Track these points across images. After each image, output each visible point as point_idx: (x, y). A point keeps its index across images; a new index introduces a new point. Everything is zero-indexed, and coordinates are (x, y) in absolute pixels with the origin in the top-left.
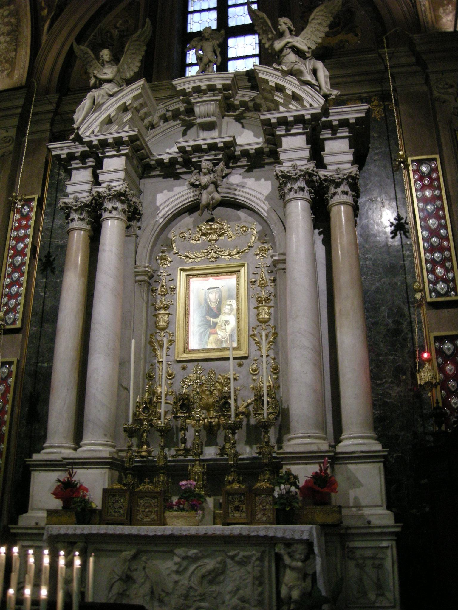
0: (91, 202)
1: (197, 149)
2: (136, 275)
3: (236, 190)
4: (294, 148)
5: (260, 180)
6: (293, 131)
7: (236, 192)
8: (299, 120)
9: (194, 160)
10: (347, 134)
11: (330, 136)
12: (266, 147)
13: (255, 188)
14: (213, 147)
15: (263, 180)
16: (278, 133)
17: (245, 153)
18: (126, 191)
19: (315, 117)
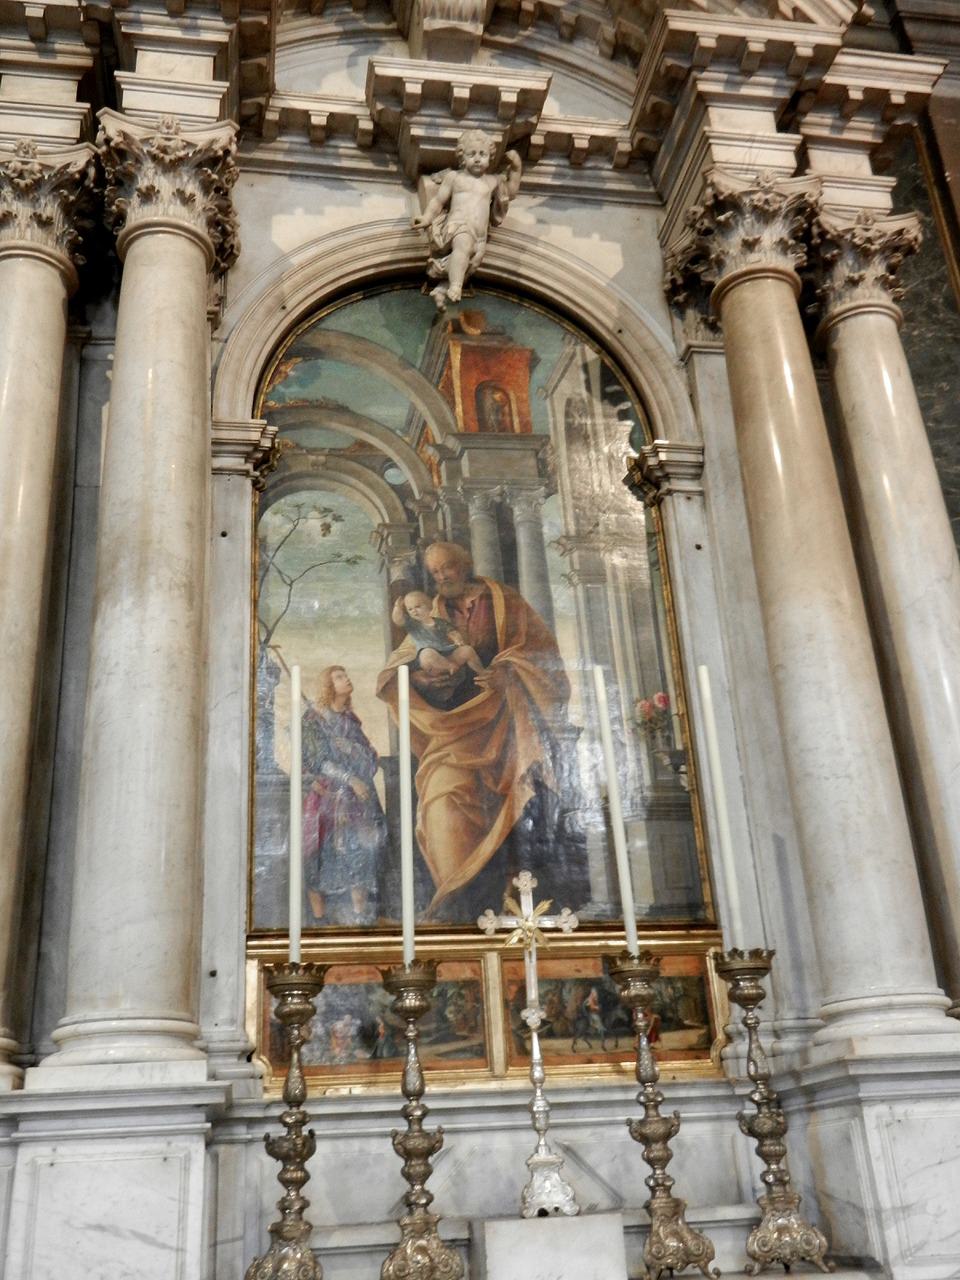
0: (84, 173)
1: (438, 95)
2: (215, 454)
3: (523, 249)
4: (745, 144)
5: (588, 235)
6: (745, 91)
7: (524, 257)
8: (779, 56)
9: (416, 131)
10: (868, 138)
11: (825, 133)
12: (623, 140)
13: (595, 254)
14: (485, 99)
15: (596, 236)
16: (702, 87)
17: (561, 145)
18: (227, 152)
19: (824, 57)
